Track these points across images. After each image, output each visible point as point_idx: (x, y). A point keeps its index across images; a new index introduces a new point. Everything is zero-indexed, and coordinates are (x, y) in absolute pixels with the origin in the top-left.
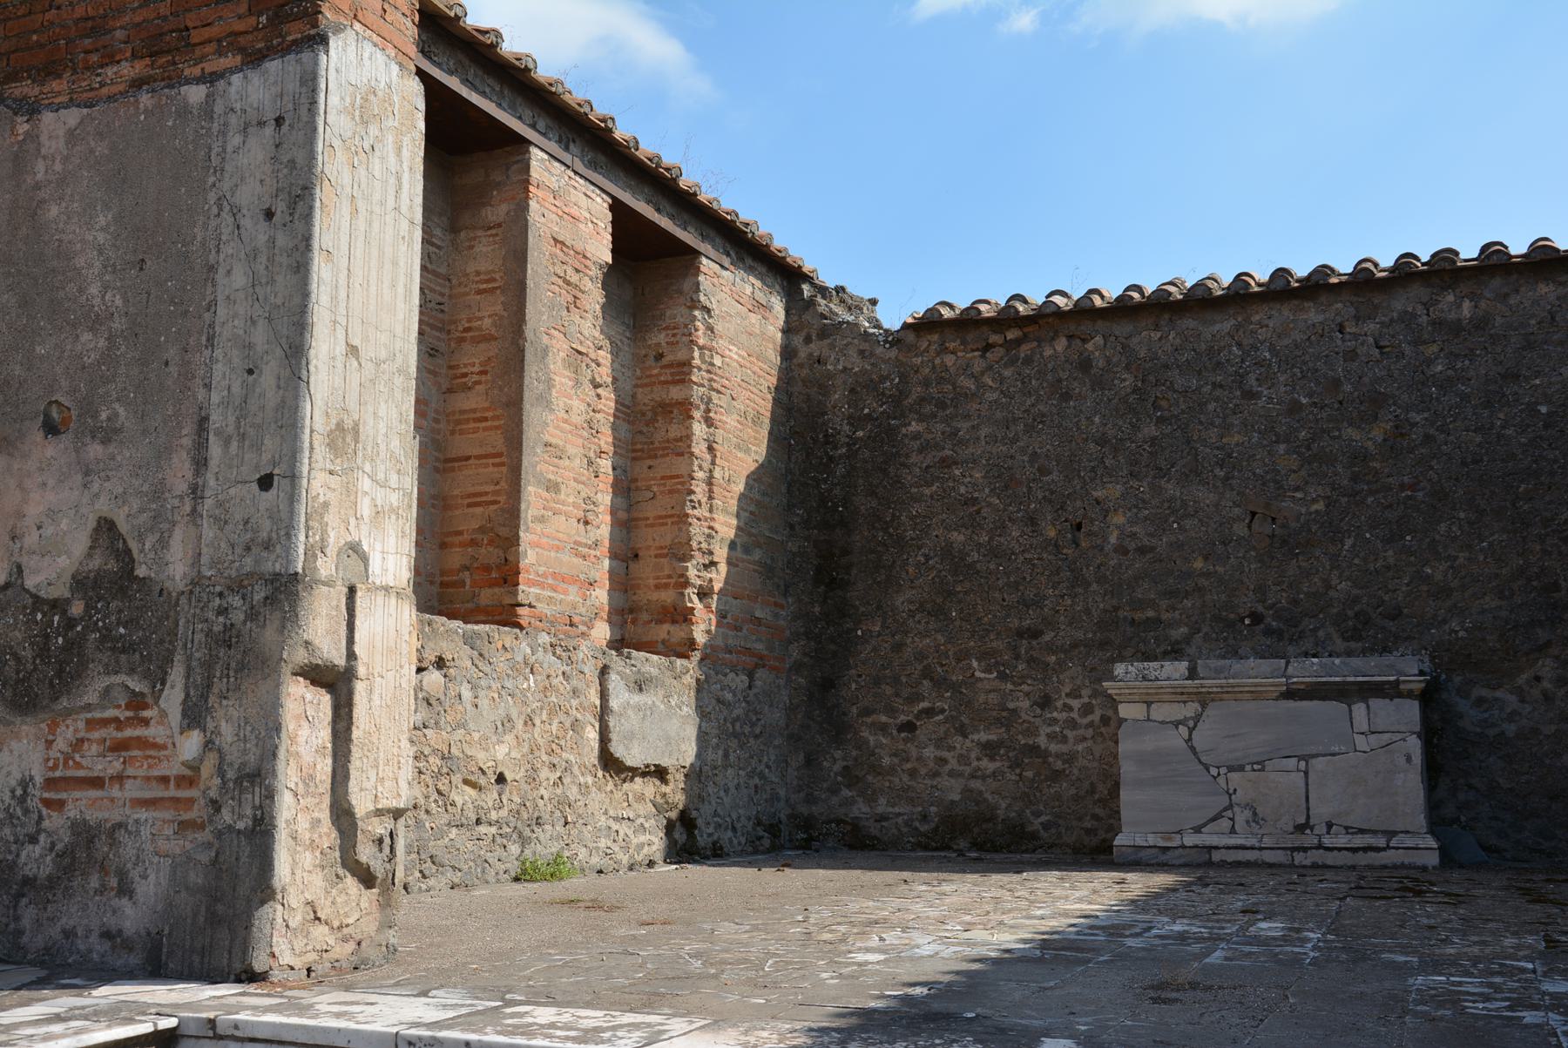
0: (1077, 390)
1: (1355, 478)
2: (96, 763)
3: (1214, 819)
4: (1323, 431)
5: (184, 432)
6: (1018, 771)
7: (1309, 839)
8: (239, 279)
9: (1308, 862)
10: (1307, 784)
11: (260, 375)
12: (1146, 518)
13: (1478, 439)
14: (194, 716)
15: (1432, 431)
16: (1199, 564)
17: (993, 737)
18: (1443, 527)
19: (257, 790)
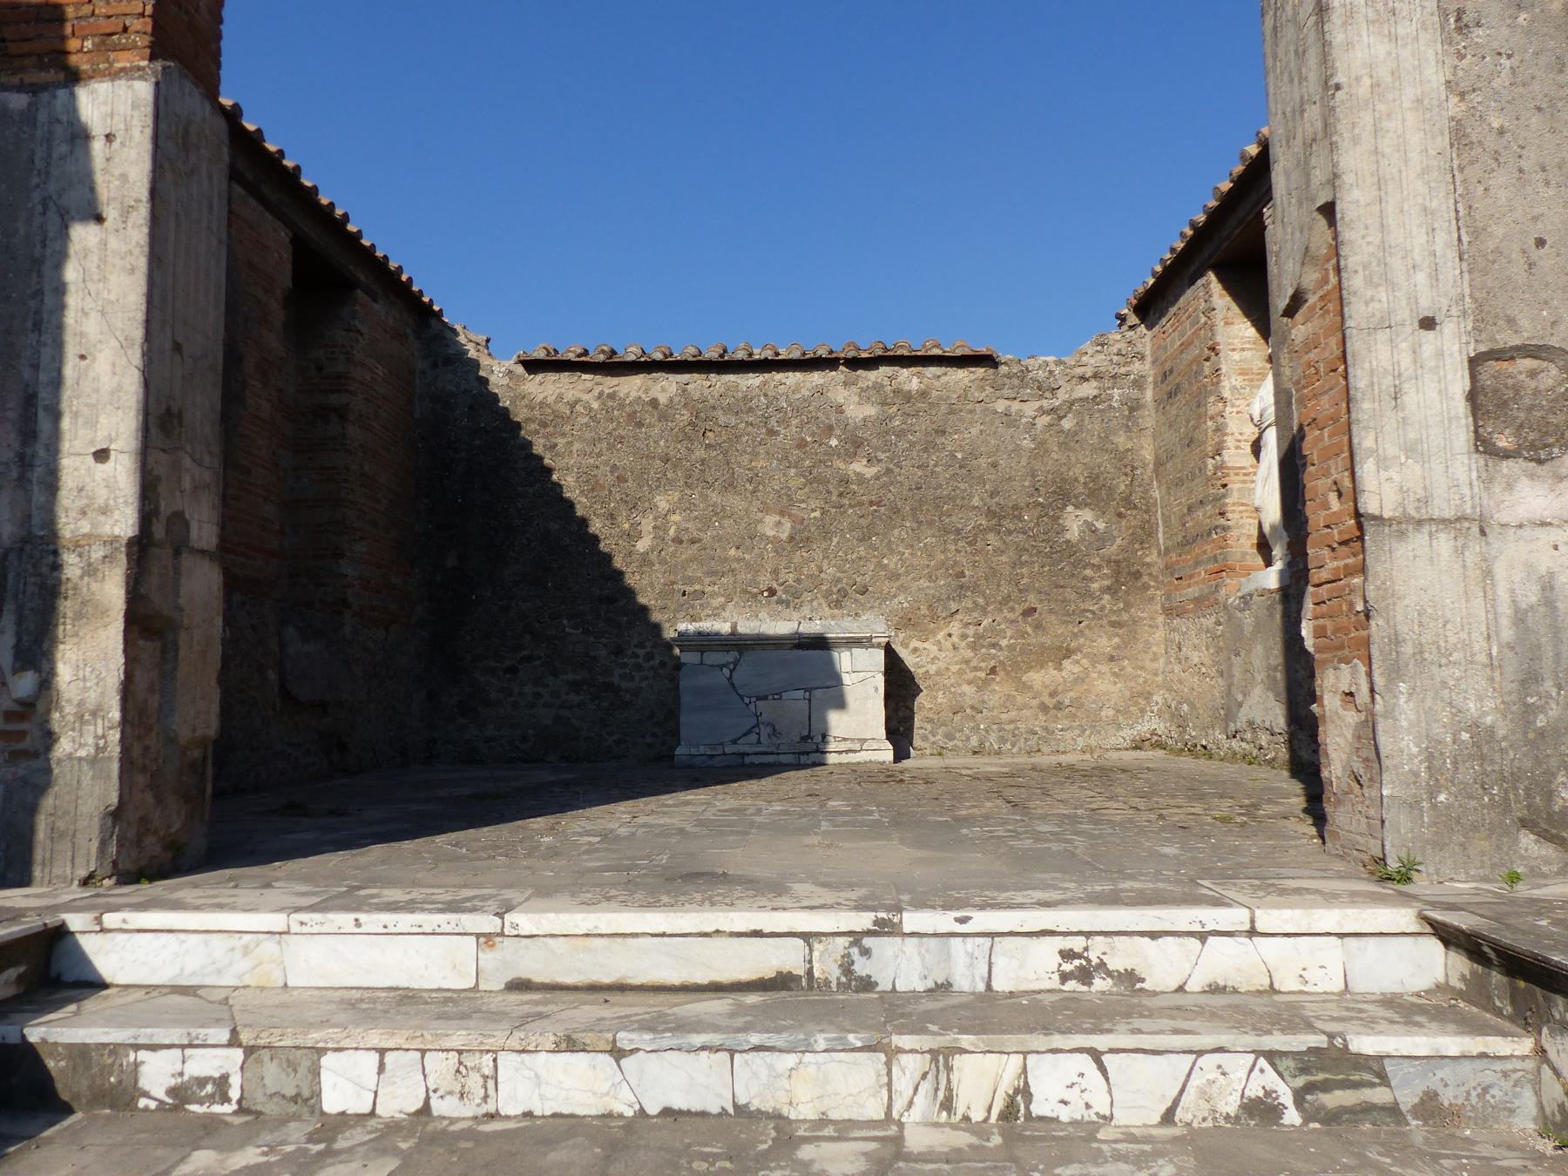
0: (648, 421)
1: (841, 495)
3: (745, 734)
4: (821, 461)
5: (10, 405)
6: (597, 702)
9: (809, 762)
10: (810, 708)
11: (94, 359)
12: (696, 518)
13: (920, 473)
15: (891, 466)
16: (733, 552)
17: (579, 677)
18: (896, 532)
19: (100, 722)
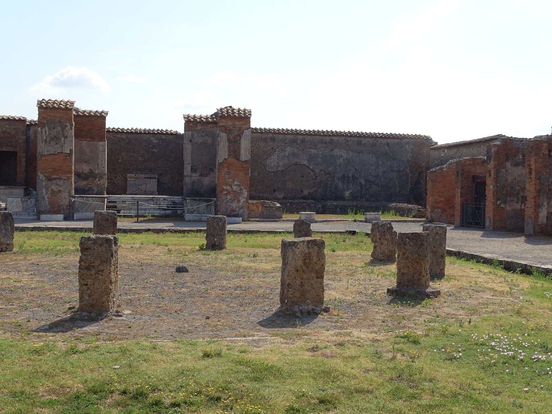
2: (90, 183)
7: (146, 192)
8: (101, 155)
16: (134, 163)
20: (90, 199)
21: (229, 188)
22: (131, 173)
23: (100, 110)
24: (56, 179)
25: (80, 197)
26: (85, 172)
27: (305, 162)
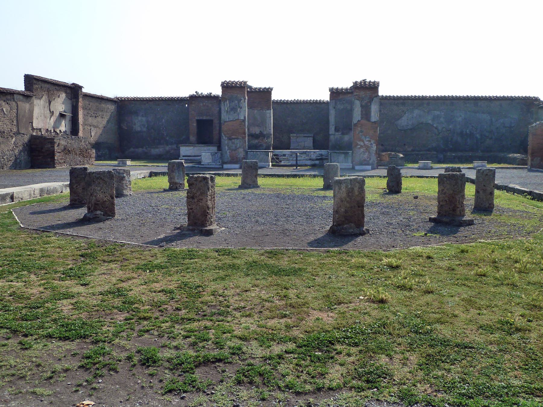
14: (267, 139)
20: (258, 153)
21: (362, 144)
22: (294, 133)
23: (267, 87)
24: (234, 139)
25: (252, 151)
26: (257, 133)
27: (430, 122)
